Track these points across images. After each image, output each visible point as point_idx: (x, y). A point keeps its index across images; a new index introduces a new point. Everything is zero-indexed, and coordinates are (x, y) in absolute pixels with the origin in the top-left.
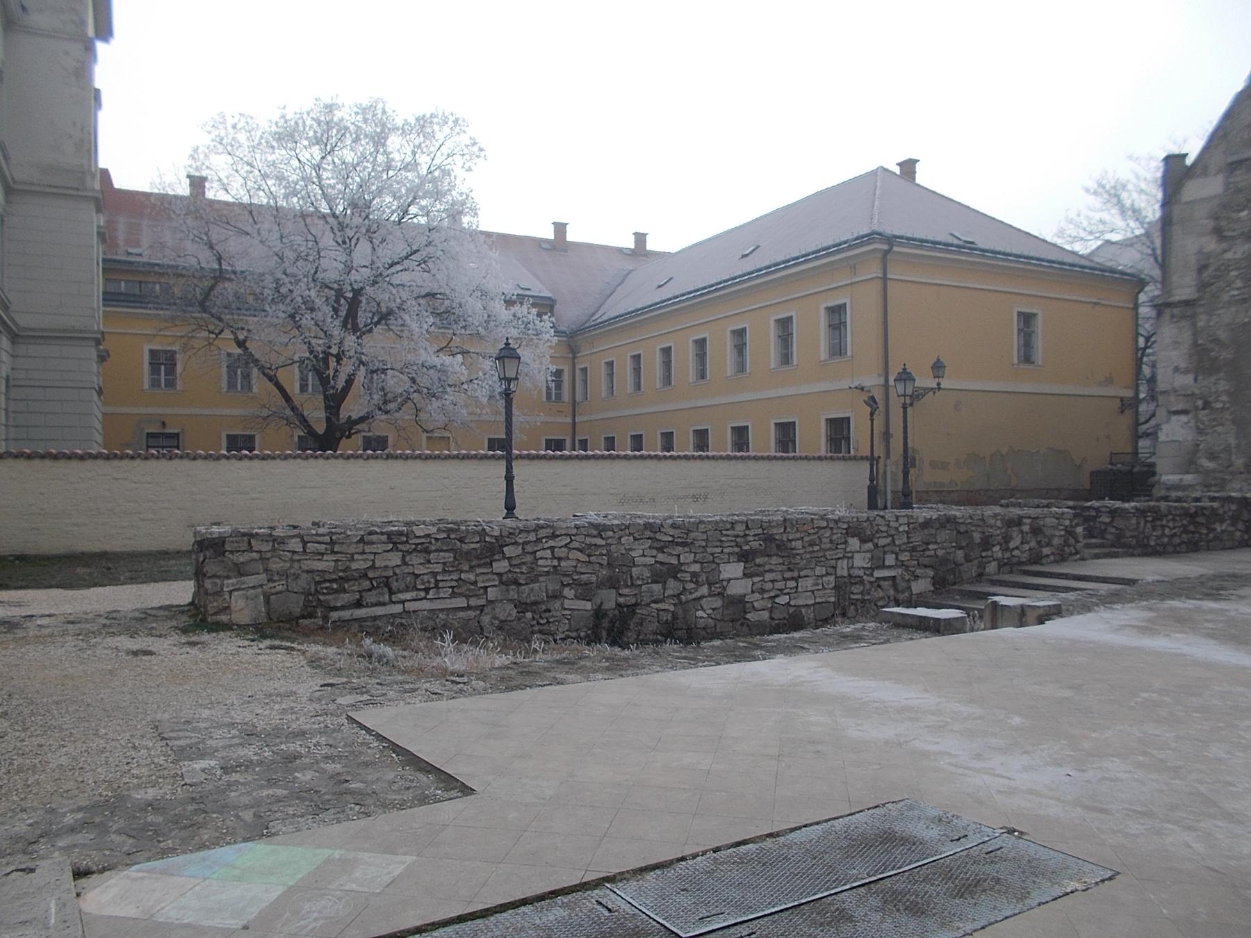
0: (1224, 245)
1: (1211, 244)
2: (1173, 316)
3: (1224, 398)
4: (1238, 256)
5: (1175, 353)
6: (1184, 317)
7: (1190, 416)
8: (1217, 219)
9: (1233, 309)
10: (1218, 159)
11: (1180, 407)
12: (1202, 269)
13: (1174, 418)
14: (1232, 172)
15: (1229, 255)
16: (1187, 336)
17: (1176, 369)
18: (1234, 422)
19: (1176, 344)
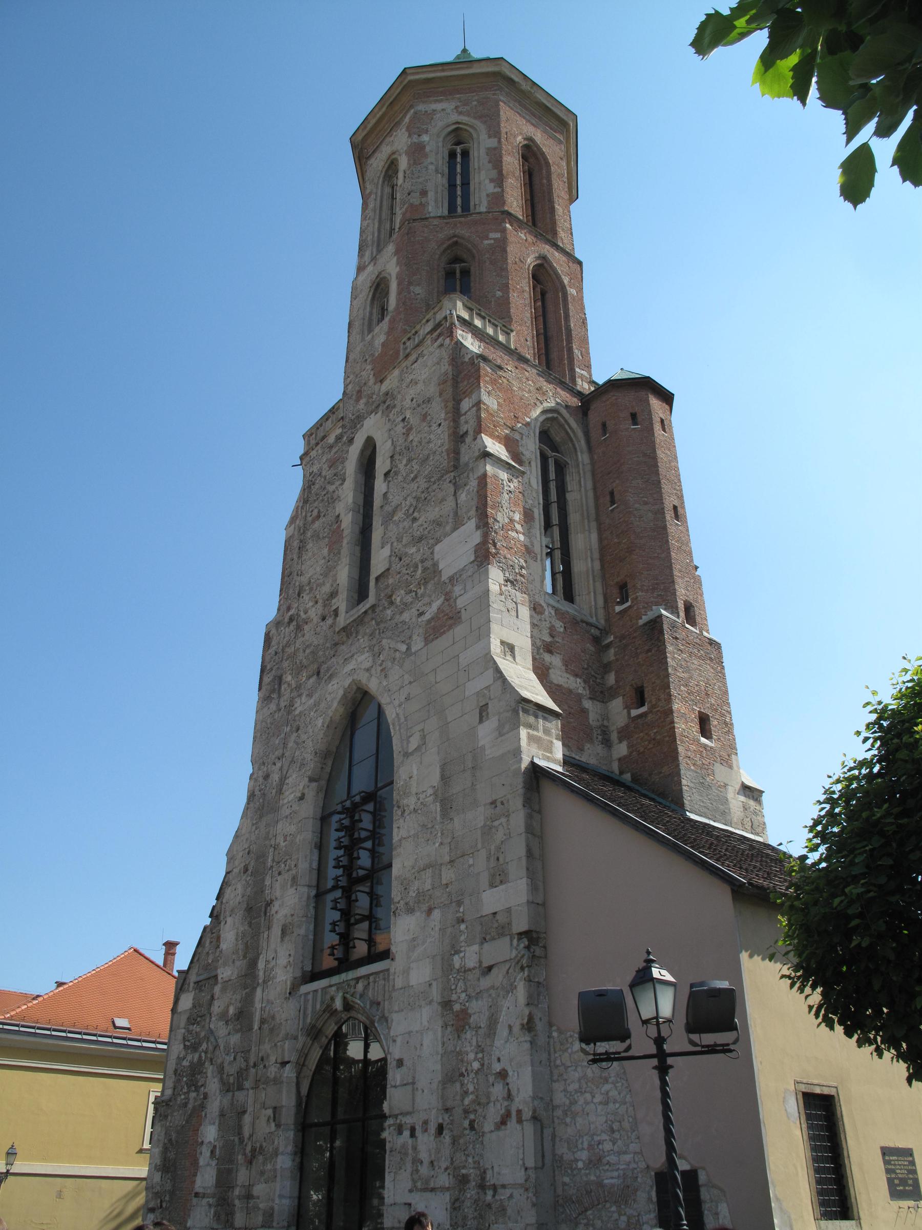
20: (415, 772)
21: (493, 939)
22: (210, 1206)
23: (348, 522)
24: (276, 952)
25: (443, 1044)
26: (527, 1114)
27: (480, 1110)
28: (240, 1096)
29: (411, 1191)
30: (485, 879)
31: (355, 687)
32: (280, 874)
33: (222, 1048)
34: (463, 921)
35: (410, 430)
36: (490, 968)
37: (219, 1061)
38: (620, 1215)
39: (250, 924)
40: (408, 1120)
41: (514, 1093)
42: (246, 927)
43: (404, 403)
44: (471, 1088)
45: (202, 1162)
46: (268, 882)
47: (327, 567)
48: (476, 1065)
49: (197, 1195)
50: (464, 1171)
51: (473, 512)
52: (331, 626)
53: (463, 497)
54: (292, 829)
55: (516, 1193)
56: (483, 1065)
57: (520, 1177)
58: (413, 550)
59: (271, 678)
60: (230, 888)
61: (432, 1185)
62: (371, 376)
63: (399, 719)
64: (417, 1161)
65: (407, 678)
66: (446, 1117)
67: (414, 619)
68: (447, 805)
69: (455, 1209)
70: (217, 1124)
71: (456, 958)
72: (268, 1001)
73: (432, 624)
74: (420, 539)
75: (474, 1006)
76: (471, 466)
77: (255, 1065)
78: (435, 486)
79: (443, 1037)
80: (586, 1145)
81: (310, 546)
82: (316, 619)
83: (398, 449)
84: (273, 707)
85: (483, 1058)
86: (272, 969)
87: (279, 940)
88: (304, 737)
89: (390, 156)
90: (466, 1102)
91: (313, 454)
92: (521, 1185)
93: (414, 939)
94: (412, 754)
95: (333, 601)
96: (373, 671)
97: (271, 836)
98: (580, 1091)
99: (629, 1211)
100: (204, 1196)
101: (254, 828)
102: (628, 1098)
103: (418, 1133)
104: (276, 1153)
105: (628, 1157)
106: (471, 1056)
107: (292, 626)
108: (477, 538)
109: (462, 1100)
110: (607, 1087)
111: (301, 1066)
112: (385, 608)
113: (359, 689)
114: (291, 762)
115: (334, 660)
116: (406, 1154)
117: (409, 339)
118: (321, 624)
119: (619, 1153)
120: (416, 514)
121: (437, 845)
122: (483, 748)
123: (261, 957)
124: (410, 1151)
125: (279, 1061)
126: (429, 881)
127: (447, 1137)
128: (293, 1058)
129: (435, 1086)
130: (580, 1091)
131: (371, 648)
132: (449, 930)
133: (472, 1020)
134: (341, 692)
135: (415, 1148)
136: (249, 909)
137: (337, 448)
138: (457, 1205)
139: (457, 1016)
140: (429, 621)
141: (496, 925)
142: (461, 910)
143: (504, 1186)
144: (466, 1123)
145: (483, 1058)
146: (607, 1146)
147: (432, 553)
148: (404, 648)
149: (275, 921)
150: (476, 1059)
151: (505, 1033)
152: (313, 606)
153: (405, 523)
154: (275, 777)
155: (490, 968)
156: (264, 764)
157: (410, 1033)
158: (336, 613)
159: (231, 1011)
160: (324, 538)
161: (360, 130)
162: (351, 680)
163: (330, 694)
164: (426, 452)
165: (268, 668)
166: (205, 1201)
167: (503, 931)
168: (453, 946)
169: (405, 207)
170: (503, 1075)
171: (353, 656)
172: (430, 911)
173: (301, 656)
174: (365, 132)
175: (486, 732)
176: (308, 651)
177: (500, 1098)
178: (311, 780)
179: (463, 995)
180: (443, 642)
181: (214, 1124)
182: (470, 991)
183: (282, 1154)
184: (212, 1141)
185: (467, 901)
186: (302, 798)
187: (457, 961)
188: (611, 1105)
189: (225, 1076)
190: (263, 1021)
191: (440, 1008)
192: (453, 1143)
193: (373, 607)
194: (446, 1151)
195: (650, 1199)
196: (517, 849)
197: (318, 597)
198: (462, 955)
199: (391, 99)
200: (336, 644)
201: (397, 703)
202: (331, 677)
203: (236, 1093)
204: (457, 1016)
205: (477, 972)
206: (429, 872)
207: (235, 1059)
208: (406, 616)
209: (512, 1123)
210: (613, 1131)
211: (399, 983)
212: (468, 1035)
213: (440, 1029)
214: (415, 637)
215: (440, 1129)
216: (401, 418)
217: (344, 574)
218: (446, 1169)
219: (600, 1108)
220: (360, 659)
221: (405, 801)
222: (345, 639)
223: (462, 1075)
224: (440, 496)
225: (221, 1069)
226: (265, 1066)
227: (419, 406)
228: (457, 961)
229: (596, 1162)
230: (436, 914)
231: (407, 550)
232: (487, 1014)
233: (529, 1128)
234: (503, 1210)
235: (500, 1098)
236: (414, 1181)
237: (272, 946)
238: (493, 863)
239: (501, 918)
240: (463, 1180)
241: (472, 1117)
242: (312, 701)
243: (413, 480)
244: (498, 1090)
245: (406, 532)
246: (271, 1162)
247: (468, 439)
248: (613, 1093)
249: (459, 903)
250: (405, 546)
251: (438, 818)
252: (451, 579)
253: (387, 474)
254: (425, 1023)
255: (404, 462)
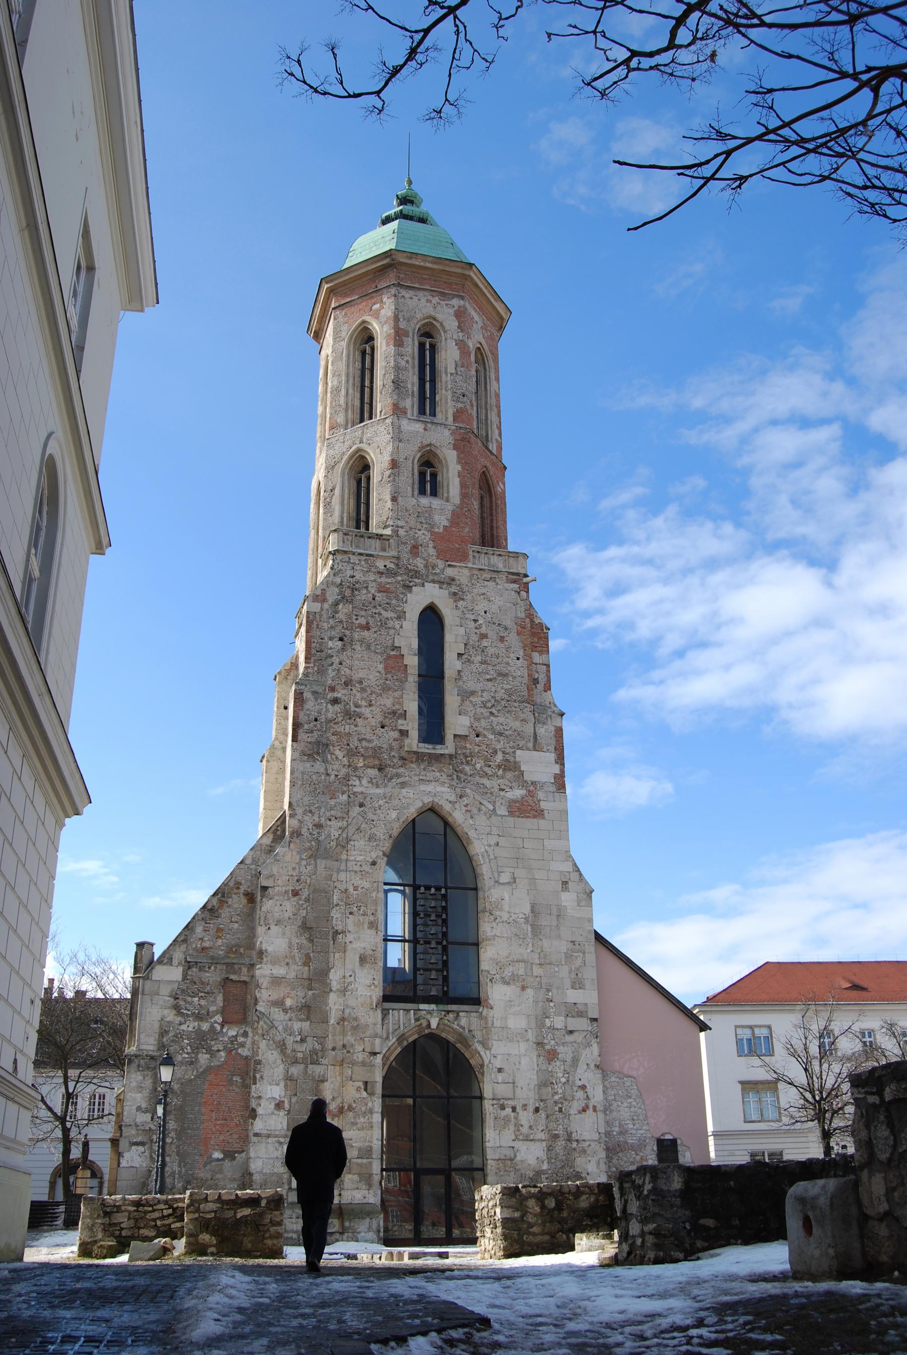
0: (179, 1019)
1: (171, 1016)
2: (139, 1066)
3: (173, 1134)
4: (190, 1029)
5: (139, 1095)
6: (148, 1068)
7: (146, 1147)
8: (176, 999)
9: (183, 1068)
10: (178, 956)
11: (139, 1139)
12: (163, 1033)
13: (133, 1148)
14: (189, 968)
15: (184, 1027)
16: (149, 1083)
17: (139, 1109)
18: (178, 1154)
19: (140, 1088)
20: (507, 898)
21: (573, 1017)
22: (281, 1143)
23: (412, 661)
24: (354, 972)
25: (538, 1065)
26: (600, 1108)
27: (567, 1103)
28: (317, 1070)
29: (514, 1140)
30: (567, 983)
31: (430, 805)
32: (351, 913)
33: (280, 1028)
34: (551, 1001)
35: (484, 636)
36: (571, 1032)
37: (278, 1038)
38: (637, 1155)
39: (311, 941)
40: (511, 1103)
41: (591, 1096)
42: (304, 942)
43: (477, 608)
44: (560, 1091)
45: (260, 1111)
46: (335, 914)
47: (384, 683)
48: (563, 1080)
49: (256, 1135)
50: (556, 1132)
51: (552, 748)
52: (395, 740)
53: (541, 731)
54: (367, 885)
55: (592, 1144)
56: (568, 1081)
57: (596, 1136)
58: (492, 737)
59: (313, 740)
60: (270, 901)
61: (532, 1138)
62: (431, 546)
63: (489, 856)
64: (518, 1126)
65: (495, 831)
66: (542, 1104)
67: (496, 789)
68: (536, 931)
69: (548, 1150)
70: (282, 1084)
71: (547, 1020)
72: (347, 1006)
73: (517, 805)
74: (501, 734)
75: (560, 1049)
76: (549, 713)
77: (334, 1049)
78: (516, 704)
79: (538, 1061)
80: (618, 1125)
81: (357, 647)
82: (373, 722)
83: (471, 642)
84: (319, 766)
85: (568, 1077)
86: (351, 983)
87: (357, 964)
88: (370, 816)
89: (428, 317)
90: (556, 1097)
91: (355, 559)
92: (596, 1141)
93: (510, 1001)
94: (503, 884)
95: (400, 722)
96: (457, 806)
97: (334, 878)
98: (615, 1100)
99: (641, 1154)
100: (269, 1136)
101: (304, 863)
102: (642, 1106)
103: (519, 1109)
104: (371, 1112)
105: (642, 1132)
106: (561, 1075)
107: (337, 708)
108: (556, 769)
109: (553, 1096)
110: (629, 1100)
111: (385, 1058)
112: (462, 763)
113: (432, 807)
114: (357, 829)
115: (401, 770)
116: (509, 1121)
117: (478, 552)
118: (382, 730)
119: (637, 1130)
120: (493, 710)
121: (529, 951)
122: (565, 907)
123: (332, 970)
124: (513, 1119)
125: (368, 1049)
126: (523, 970)
127: (543, 1115)
128: (384, 1052)
129: (532, 1087)
130: (615, 1100)
131: (451, 786)
132: (541, 1004)
133: (560, 1056)
134: (419, 804)
135: (516, 1118)
136: (305, 927)
137: (389, 580)
138: (551, 1148)
139: (549, 1052)
140: (515, 801)
141: (576, 1010)
142: (550, 994)
143: (584, 1141)
144: (557, 1108)
145: (568, 1077)
146: (631, 1126)
147: (514, 752)
148: (491, 808)
149: (349, 947)
150: (563, 1077)
151: (585, 1067)
152: (366, 706)
153: (482, 710)
154: (335, 833)
155: (571, 1032)
156: (310, 811)
157: (509, 1054)
158: (404, 733)
159: (289, 1002)
160: (376, 653)
161: (405, 255)
162: (431, 799)
163: (404, 797)
164: (505, 671)
165: (306, 727)
166: (270, 1140)
167: (581, 1014)
168: (544, 1013)
169: (460, 405)
170: (583, 1087)
171: (431, 781)
172: (523, 988)
173: (354, 742)
174: (406, 261)
175: (568, 899)
176: (364, 744)
177: (582, 1098)
178: (384, 854)
179: (553, 1042)
180: (529, 823)
181: (278, 1085)
182: (557, 1040)
183: (377, 1112)
184: (278, 1098)
185: (554, 991)
186: (374, 863)
187: (548, 1022)
188: (633, 1109)
189: (289, 1052)
190: (343, 1019)
191: (535, 1045)
192: (547, 1117)
193: (451, 756)
194: (543, 1121)
195: (653, 1150)
196: (590, 974)
197: (373, 702)
198: (552, 1019)
199: (448, 269)
200: (405, 760)
201: (486, 843)
202: (403, 785)
203: (310, 1066)
204: (549, 1052)
205: (564, 1032)
206: (522, 965)
207: (303, 1040)
208: (485, 781)
209: (590, 1111)
210: (633, 1120)
211: (497, 1023)
212: (558, 1063)
213: (535, 1057)
214: (498, 804)
215: (537, 1110)
216: (472, 617)
217: (412, 705)
218: (542, 1131)
219: (626, 1109)
220: (439, 789)
221: (498, 913)
222: (414, 760)
223: (552, 1083)
224: (522, 716)
225: (281, 1046)
226: (348, 1052)
227: (494, 624)
228: (548, 1022)
229: (623, 1132)
230: (530, 992)
231: (486, 733)
232: (571, 1055)
233: (601, 1115)
234: (584, 1151)
235: (582, 1098)
236: (516, 1136)
237: (349, 966)
238: (573, 976)
239: (580, 1007)
240: (556, 1136)
241: (560, 1106)
242: (378, 791)
243: (488, 680)
244: (580, 1094)
245: (484, 718)
246: (364, 1117)
247: (540, 687)
248: (634, 1103)
249: (548, 990)
250: (484, 728)
251: (530, 935)
252: (533, 783)
253: (460, 655)
254: (522, 1050)
255: (479, 658)
